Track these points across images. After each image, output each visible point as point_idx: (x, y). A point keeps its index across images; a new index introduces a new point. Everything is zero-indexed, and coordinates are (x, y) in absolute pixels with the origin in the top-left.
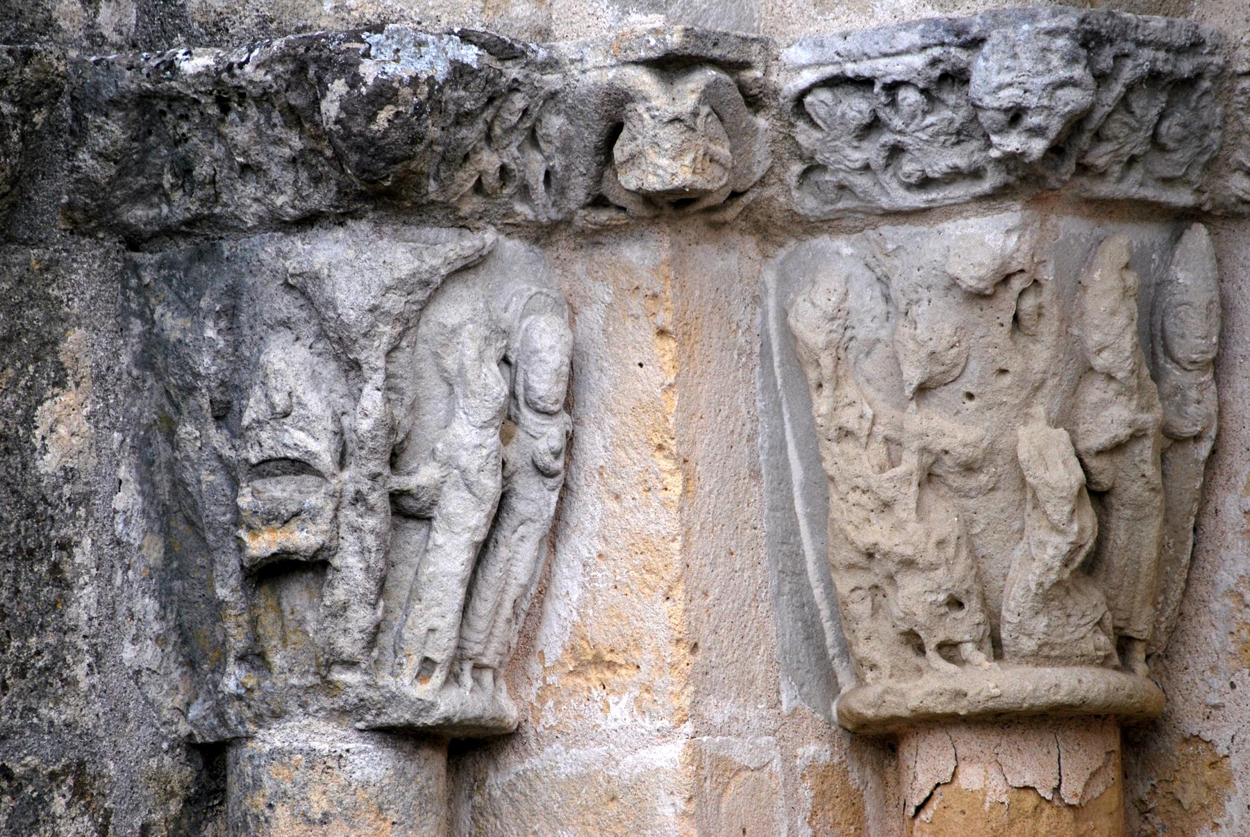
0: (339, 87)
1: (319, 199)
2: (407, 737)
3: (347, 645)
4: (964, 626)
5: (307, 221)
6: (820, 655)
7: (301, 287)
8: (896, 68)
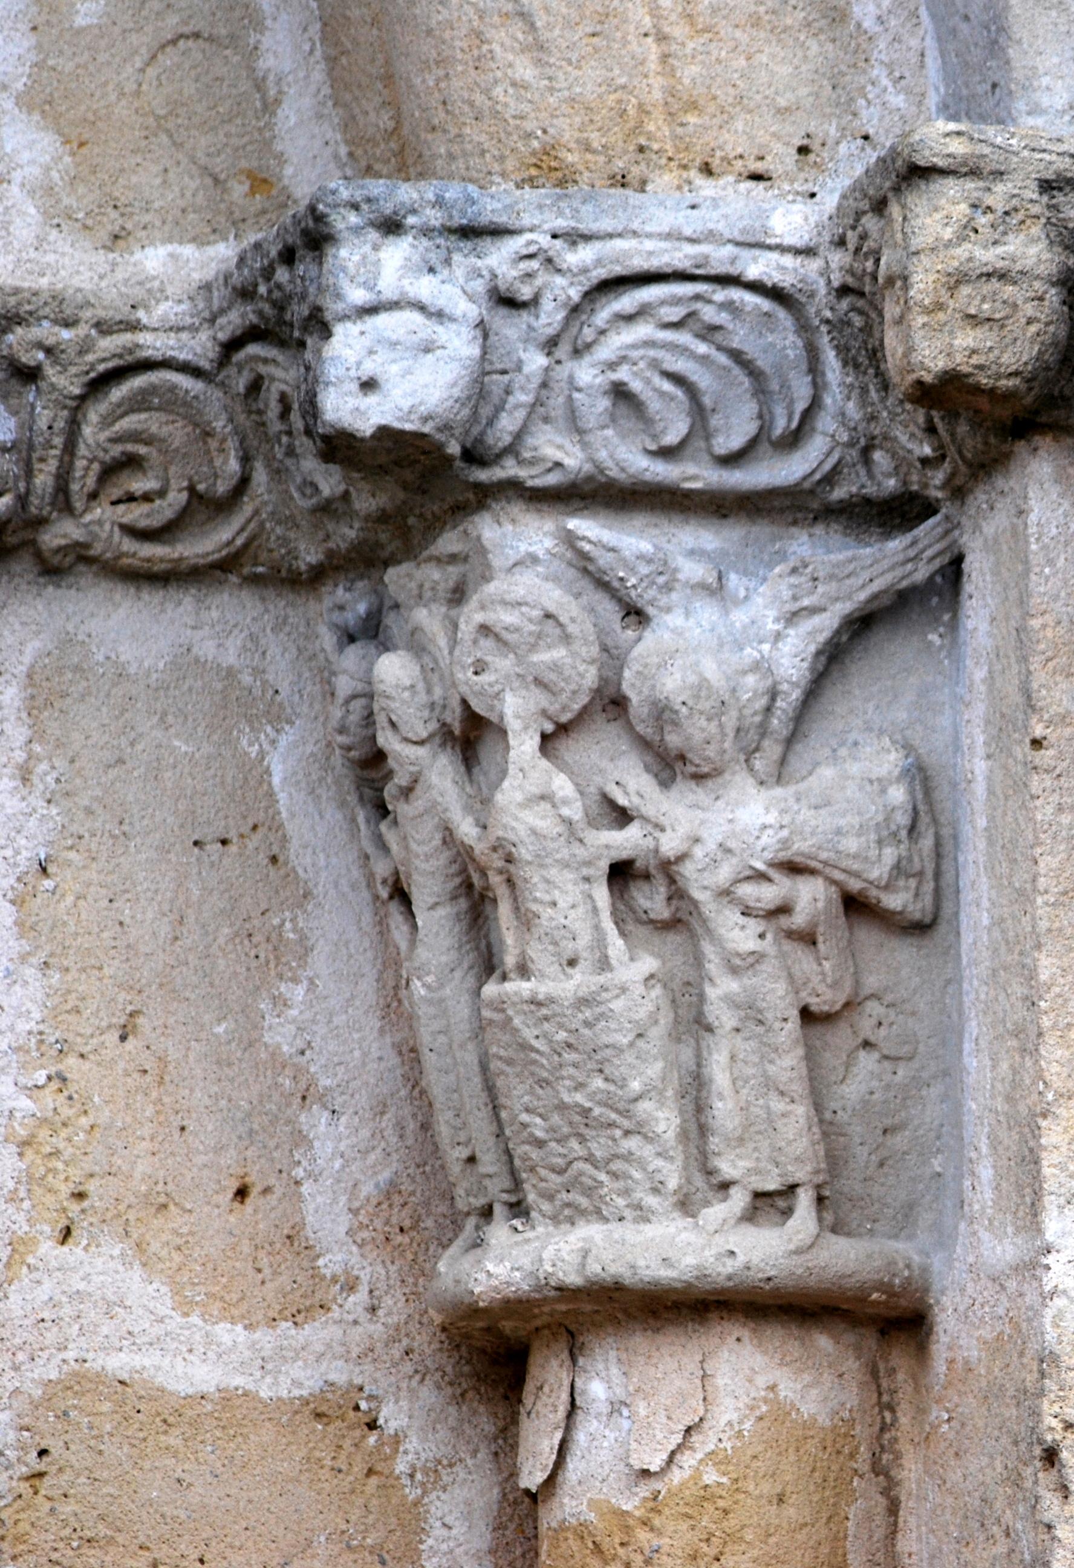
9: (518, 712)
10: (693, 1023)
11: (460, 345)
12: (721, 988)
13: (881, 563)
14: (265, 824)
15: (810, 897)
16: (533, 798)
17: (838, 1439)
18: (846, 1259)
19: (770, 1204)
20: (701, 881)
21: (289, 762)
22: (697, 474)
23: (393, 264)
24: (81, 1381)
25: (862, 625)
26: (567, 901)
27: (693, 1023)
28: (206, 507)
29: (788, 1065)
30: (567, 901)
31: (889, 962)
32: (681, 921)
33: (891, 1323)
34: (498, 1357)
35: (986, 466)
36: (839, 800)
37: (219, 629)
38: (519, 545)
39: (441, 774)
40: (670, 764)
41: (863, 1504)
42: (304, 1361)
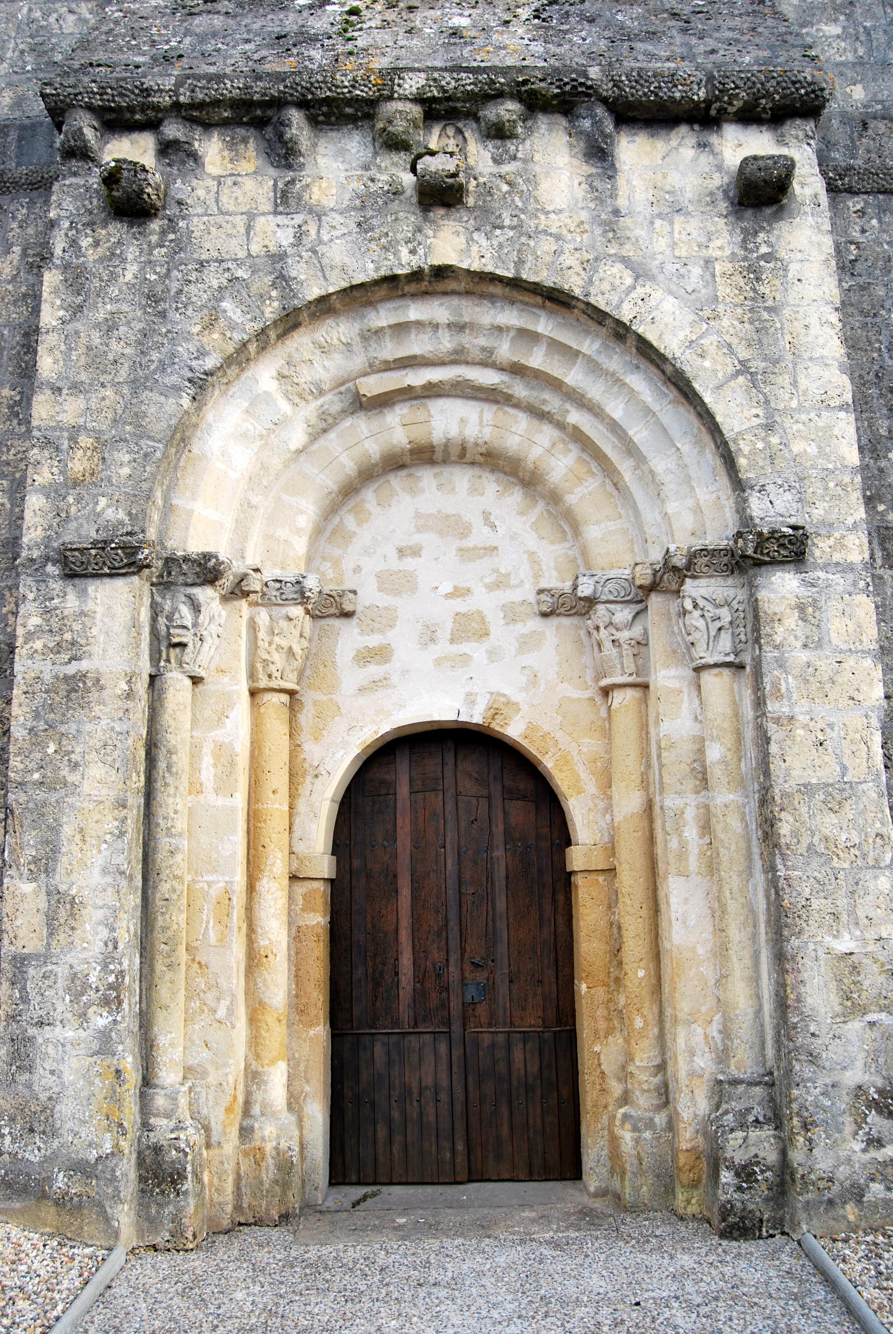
0: (214, 560)
1: (198, 581)
2: (191, 677)
3: (187, 661)
4: (278, 675)
5: (193, 585)
6: (252, 675)
7: (189, 597)
8: (288, 580)
9: (602, 626)
10: (621, 656)
11: (592, 587)
12: (624, 653)
13: (639, 607)
14: (581, 640)
15: (633, 642)
16: (603, 634)
17: (640, 699)
18: (639, 680)
19: (631, 675)
20: (621, 641)
21: (582, 633)
22: (619, 599)
23: (585, 579)
24: (564, 697)
25: (638, 613)
26: (607, 644)
27: (621, 656)
28: (572, 608)
29: (632, 660)
30: (607, 644)
31: (643, 649)
32: (620, 646)
33: (646, 687)
34: (606, 692)
35: (648, 595)
36: (636, 632)
37: (574, 620)
38: (601, 608)
39: (595, 632)
40: (617, 630)
41: (644, 705)
42: (588, 694)
